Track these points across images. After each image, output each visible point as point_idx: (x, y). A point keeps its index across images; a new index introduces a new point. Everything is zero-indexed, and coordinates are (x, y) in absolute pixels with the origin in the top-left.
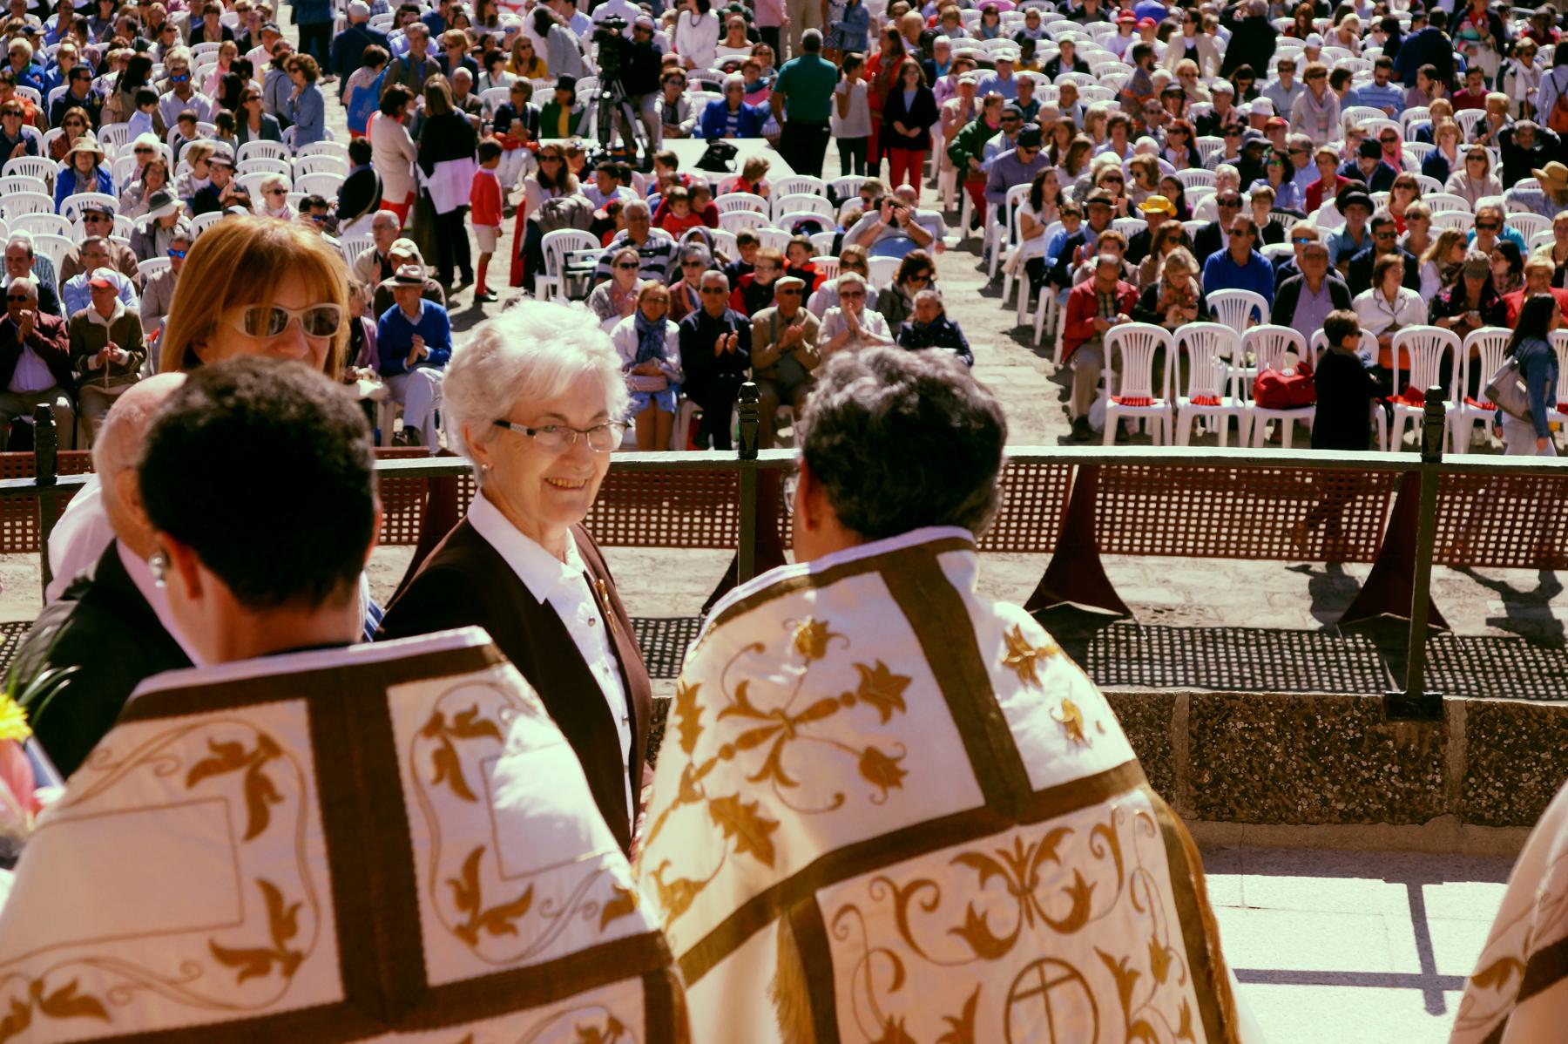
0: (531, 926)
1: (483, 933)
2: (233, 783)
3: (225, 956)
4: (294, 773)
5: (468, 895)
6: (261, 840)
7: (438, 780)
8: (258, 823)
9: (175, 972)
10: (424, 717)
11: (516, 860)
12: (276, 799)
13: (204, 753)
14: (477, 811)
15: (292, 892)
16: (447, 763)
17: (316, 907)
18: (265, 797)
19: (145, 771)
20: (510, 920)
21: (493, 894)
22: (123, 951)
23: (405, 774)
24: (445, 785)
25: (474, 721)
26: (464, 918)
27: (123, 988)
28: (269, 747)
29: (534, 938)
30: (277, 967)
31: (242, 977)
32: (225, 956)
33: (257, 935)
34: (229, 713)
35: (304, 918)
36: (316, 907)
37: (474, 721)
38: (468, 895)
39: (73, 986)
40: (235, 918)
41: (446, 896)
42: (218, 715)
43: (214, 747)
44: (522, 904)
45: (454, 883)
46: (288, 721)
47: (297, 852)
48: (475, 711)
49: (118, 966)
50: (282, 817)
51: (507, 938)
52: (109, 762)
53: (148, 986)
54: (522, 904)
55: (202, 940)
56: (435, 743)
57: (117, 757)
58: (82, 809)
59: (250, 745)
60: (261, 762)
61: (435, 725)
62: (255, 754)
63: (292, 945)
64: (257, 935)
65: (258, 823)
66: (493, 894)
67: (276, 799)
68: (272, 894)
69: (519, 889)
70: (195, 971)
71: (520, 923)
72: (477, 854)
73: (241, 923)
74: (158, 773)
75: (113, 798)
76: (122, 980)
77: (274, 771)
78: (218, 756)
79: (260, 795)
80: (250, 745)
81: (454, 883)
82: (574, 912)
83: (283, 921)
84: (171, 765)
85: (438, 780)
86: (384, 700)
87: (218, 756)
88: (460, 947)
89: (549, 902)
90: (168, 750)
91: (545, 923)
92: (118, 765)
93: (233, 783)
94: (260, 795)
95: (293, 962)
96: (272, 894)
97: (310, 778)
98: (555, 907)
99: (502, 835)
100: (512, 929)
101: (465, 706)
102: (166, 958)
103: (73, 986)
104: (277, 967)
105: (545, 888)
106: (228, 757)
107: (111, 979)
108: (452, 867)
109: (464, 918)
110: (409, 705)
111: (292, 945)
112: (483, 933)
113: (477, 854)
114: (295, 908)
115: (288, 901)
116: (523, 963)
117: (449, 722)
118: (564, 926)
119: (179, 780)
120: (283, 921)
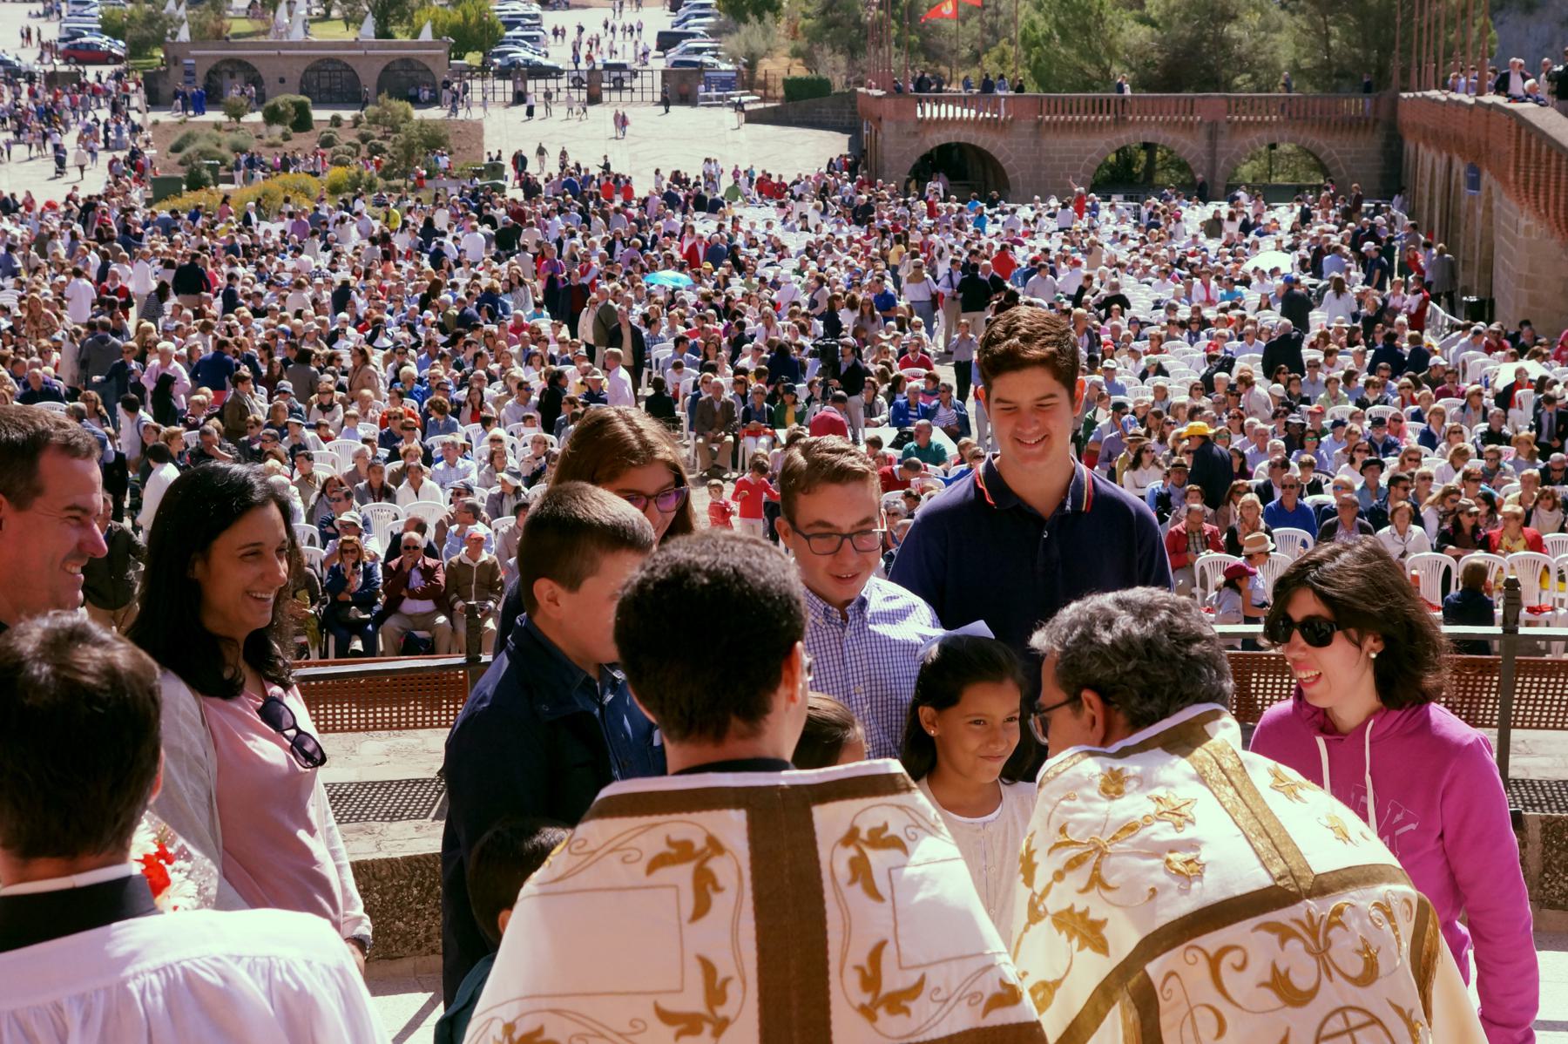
0: (921, 1008)
1: (881, 1012)
2: (683, 874)
3: (666, 1017)
4: (734, 869)
5: (871, 980)
6: (703, 923)
7: (853, 881)
8: (701, 909)
9: (627, 1029)
10: (842, 830)
11: (913, 951)
12: (718, 889)
13: (663, 847)
14: (881, 912)
15: (725, 968)
16: (860, 871)
17: (744, 982)
18: (709, 887)
19: (614, 858)
20: (904, 1003)
21: (893, 981)
22: (582, 1005)
23: (826, 875)
24: (858, 888)
25: (883, 836)
26: (866, 999)
27: (581, 1037)
28: (715, 846)
29: (923, 1020)
30: (708, 1029)
31: (678, 1035)
32: (666, 1017)
33: (693, 1001)
34: (685, 816)
35: (733, 990)
36: (744, 982)
37: (883, 836)
38: (871, 980)
39: (540, 1031)
40: (678, 987)
41: (853, 980)
42: (675, 817)
43: (670, 843)
44: (915, 991)
45: (860, 968)
46: (732, 826)
47: (731, 934)
48: (885, 827)
49: (577, 1017)
50: (722, 904)
51: (902, 1017)
52: (586, 849)
53: (602, 1036)
54: (915, 991)
55: (648, 1002)
56: (852, 852)
57: (592, 846)
58: (560, 886)
59: (700, 843)
60: (708, 858)
61: (851, 837)
62: (703, 851)
63: (721, 1012)
64: (693, 1001)
65: (701, 909)
66: (893, 981)
67: (718, 889)
68: (708, 968)
69: (914, 977)
70: (641, 1026)
71: (913, 1006)
72: (881, 945)
73: (681, 991)
74: (623, 860)
75: (584, 879)
76: (582, 1029)
77: (717, 865)
78: (673, 851)
79: (705, 885)
80: (700, 843)
81: (860, 968)
82: (959, 999)
83: (715, 992)
84: (635, 855)
85: (853, 881)
86: (810, 816)
87: (673, 851)
88: (861, 1022)
89: (938, 989)
90: (633, 843)
91: (934, 1008)
92: (594, 852)
93: (683, 874)
94: (705, 885)
95: (721, 1026)
96: (708, 968)
97: (747, 874)
98: (943, 995)
99: (900, 931)
100: (907, 1011)
101: (880, 824)
102: (616, 1014)
103: (540, 1031)
104: (708, 1029)
105: (934, 978)
106: (681, 852)
107: (572, 1028)
108: (860, 955)
109: (866, 999)
110: (829, 819)
111: (721, 1012)
112: (881, 1012)
113: (881, 945)
114: (727, 981)
115: (721, 975)
116: (913, 1040)
117: (864, 835)
118: (950, 1010)
119: (641, 867)
120: (715, 992)
